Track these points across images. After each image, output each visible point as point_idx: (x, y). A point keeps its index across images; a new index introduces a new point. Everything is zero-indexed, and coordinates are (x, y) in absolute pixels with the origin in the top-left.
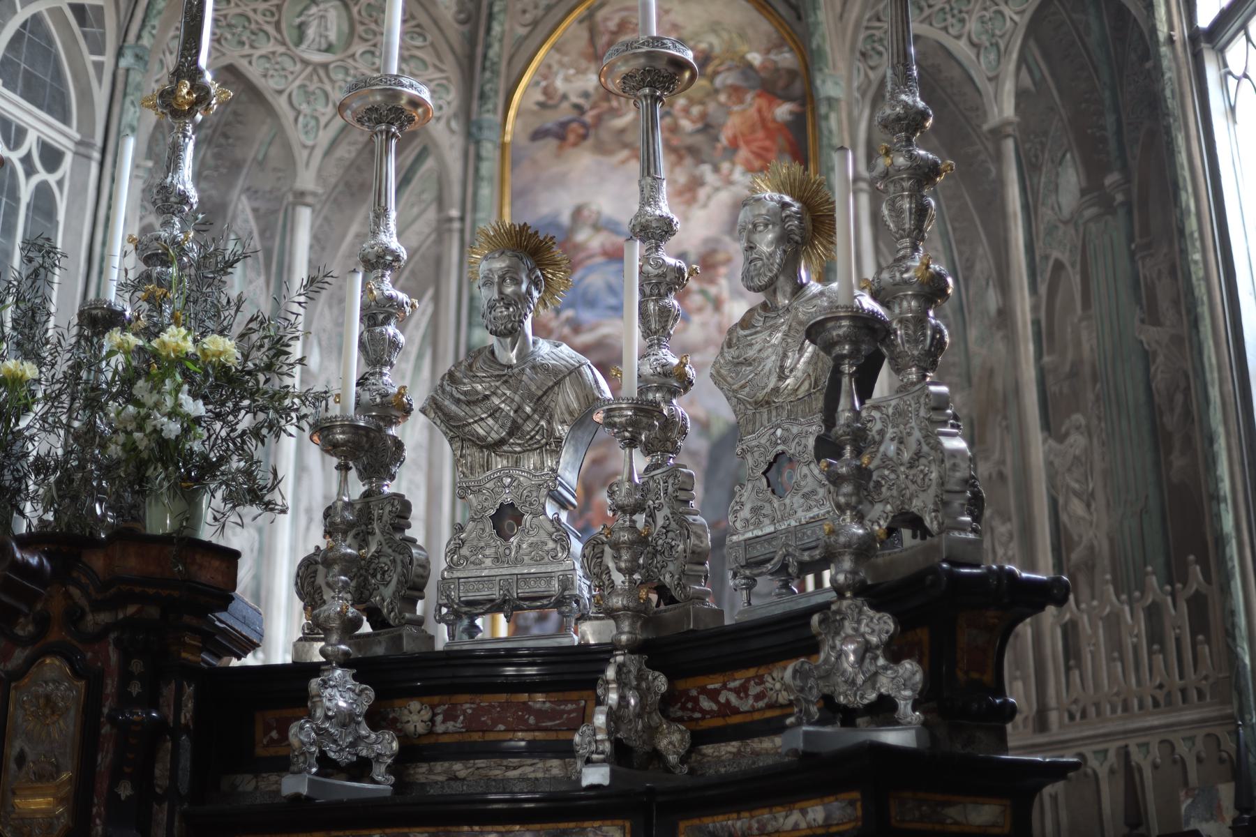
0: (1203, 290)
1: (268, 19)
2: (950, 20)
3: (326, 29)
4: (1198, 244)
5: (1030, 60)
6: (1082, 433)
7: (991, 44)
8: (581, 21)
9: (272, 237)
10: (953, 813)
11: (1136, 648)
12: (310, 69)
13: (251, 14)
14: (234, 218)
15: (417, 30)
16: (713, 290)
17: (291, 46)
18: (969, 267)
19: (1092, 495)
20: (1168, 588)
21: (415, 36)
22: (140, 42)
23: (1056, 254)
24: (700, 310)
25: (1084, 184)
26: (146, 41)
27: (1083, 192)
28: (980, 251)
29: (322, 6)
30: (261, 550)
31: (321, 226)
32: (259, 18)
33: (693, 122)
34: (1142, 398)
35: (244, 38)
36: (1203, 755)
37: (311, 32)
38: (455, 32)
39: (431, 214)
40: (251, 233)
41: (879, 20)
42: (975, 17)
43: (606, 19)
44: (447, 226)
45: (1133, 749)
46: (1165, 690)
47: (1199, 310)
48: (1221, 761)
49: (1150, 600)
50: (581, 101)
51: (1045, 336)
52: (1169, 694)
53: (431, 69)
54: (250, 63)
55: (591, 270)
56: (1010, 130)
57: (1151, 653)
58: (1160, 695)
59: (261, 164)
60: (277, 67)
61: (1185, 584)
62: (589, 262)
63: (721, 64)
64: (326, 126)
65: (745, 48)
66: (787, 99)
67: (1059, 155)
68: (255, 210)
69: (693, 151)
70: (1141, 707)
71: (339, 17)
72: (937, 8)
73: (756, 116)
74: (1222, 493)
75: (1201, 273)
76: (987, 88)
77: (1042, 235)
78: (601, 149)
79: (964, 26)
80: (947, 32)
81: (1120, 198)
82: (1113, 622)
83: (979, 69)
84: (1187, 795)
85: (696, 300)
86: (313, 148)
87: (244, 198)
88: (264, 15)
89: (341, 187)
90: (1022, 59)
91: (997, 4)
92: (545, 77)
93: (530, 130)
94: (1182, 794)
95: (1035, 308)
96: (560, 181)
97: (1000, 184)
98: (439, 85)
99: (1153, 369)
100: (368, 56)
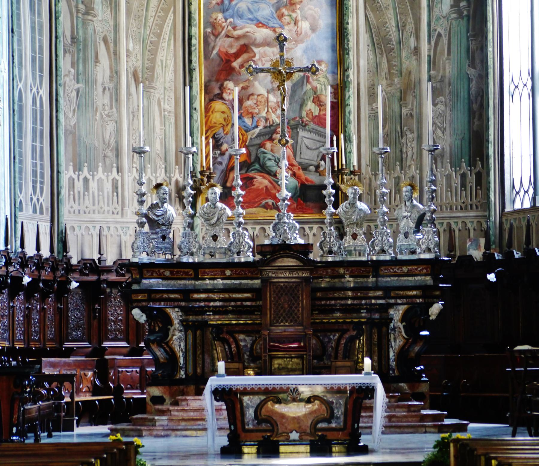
0: (492, 63)
4: (492, 44)
10: (434, 293)
11: (456, 188)
16: (294, 15)
18: (404, 26)
19: (445, 129)
20: (469, 168)
23: (439, 30)
24: (289, 24)
25: (452, 3)
27: (452, 6)
28: (409, 20)
34: (466, 96)
36: (476, 228)
45: (453, 224)
46: (465, 204)
47: (489, 70)
48: (482, 230)
49: (462, 172)
51: (432, 63)
52: (466, 206)
57: (461, 190)
58: (463, 206)
61: (475, 168)
70: (456, 209)
74: (490, 140)
75: (492, 56)
77: (434, 20)
81: (465, 13)
82: (449, 177)
84: (469, 241)
85: (287, 19)
94: (468, 240)
95: (429, 50)
99: (471, 86)
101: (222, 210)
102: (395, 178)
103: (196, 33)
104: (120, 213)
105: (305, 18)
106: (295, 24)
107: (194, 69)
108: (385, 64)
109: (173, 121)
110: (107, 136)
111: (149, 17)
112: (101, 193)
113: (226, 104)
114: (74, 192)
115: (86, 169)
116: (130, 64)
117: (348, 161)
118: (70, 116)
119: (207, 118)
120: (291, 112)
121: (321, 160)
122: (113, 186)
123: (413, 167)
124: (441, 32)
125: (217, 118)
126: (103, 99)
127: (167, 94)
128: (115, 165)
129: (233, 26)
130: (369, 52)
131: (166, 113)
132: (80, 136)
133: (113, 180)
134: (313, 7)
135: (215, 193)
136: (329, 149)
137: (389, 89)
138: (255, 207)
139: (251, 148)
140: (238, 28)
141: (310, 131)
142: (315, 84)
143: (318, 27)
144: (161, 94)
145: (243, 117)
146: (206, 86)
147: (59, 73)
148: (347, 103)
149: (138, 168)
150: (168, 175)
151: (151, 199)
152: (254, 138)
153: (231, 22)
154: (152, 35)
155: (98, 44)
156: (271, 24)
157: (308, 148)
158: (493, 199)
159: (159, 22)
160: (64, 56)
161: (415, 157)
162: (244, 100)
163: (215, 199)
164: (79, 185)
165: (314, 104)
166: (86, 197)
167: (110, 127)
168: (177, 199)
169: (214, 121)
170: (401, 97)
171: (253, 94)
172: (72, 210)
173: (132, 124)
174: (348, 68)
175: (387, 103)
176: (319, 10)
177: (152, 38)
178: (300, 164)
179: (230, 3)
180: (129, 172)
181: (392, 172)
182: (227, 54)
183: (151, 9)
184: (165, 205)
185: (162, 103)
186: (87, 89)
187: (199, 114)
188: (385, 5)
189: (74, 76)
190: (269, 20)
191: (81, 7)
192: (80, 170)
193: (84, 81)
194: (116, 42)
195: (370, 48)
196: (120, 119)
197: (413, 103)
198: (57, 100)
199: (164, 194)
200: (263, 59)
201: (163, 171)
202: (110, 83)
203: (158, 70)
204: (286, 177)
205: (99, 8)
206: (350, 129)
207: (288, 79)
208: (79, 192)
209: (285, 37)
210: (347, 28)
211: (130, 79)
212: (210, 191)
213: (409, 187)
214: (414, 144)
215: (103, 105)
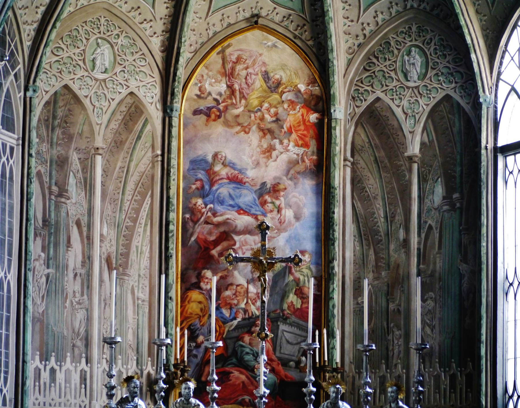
0: (485, 258)
1: (80, 58)
2: (395, 97)
3: (104, 61)
4: (485, 239)
5: (429, 130)
6: (432, 301)
7: (412, 116)
8: (218, 53)
9: (87, 172)
11: (445, 390)
12: (98, 82)
13: (73, 56)
14: (71, 164)
15: (142, 56)
17: (90, 71)
18: (393, 217)
19: (434, 327)
20: (459, 369)
22: (35, 84)
23: (430, 222)
24: (271, 211)
25: (444, 194)
26: (38, 83)
27: (444, 198)
28: (398, 211)
29: (102, 48)
30: (87, 319)
31: (106, 165)
33: (272, 117)
34: (457, 293)
35: (71, 70)
37: (98, 63)
38: (159, 56)
39: (150, 154)
40: (78, 171)
41: (362, 83)
42: (406, 99)
43: (231, 54)
44: (156, 159)
47: (482, 266)
50: (218, 97)
51: (422, 256)
54: (74, 83)
55: (222, 185)
56: (416, 159)
57: (450, 392)
59: (80, 135)
60: (85, 83)
62: (220, 182)
63: (286, 88)
64: (106, 113)
65: (297, 81)
66: (316, 111)
67: (436, 178)
68: (79, 159)
71: (109, 53)
72: (390, 88)
73: (301, 117)
74: (482, 340)
75: (485, 251)
76: (409, 136)
77: (425, 212)
78: (227, 124)
79: (401, 102)
80: (393, 101)
81: (458, 205)
82: (437, 378)
83: (407, 127)
85: (270, 206)
86: (101, 124)
87: (74, 153)
88: (78, 56)
89: (113, 144)
90: (425, 128)
91: (417, 97)
92: (200, 82)
93: (193, 109)
95: (419, 243)
96: (207, 138)
97: (409, 183)
100: (122, 73)
101: (195, 406)
102: (380, 377)
103: (174, 219)
106: (278, 212)
107: (171, 256)
108: (372, 257)
109: (147, 310)
110: (77, 325)
111: (125, 201)
112: (68, 385)
113: (203, 294)
114: (39, 383)
115: (53, 359)
116: (104, 249)
117: (330, 357)
118: (39, 302)
119: (183, 308)
120: (271, 304)
121: (302, 356)
122: (81, 378)
123: (400, 366)
124: (431, 223)
125: (193, 308)
126: (74, 285)
127: (142, 281)
128: (84, 355)
129: (213, 212)
130: (356, 243)
131: (140, 302)
132: (48, 324)
133: (81, 371)
134: (297, 195)
135: (189, 388)
136: (310, 344)
137: (376, 282)
138: (231, 404)
139: (228, 341)
140: (218, 214)
141: (291, 325)
142: (298, 275)
143: (303, 215)
144: (136, 282)
145: (221, 308)
146: (182, 274)
147: (28, 257)
148: (331, 296)
149: (108, 359)
150: (140, 367)
151: (121, 393)
152: (232, 330)
153: (210, 208)
154: (127, 220)
155: (71, 228)
156: (253, 211)
157: (288, 342)
158: (484, 403)
159: (136, 206)
160: (35, 240)
161: (401, 355)
162: (222, 290)
163: (189, 394)
164: (45, 376)
165: (296, 297)
166: (53, 389)
167: (81, 315)
168: (149, 393)
169: (190, 311)
170: (388, 291)
171: (232, 284)
172: (37, 402)
173: (104, 312)
174: (333, 259)
175: (373, 297)
176: (304, 198)
177: (128, 222)
178: (279, 359)
179: (210, 189)
180: (99, 363)
181: (378, 371)
182: (206, 241)
183: (127, 192)
184: (136, 399)
185: (136, 291)
186: (58, 275)
187: (174, 303)
188: (373, 195)
189: (44, 261)
190: (251, 207)
191: (55, 188)
192: (47, 360)
193: (54, 266)
194: (90, 226)
195: (357, 239)
196: (91, 307)
197: (400, 298)
198: (25, 286)
199: (134, 388)
200: (243, 247)
201: (135, 363)
202: (82, 269)
203: (133, 256)
204: (265, 373)
205: (73, 190)
206: (334, 323)
207: (269, 269)
208: (45, 383)
209: (267, 226)
210: (333, 218)
211: (103, 265)
212: (184, 386)
213: (395, 388)
214: (401, 341)
215: (74, 292)
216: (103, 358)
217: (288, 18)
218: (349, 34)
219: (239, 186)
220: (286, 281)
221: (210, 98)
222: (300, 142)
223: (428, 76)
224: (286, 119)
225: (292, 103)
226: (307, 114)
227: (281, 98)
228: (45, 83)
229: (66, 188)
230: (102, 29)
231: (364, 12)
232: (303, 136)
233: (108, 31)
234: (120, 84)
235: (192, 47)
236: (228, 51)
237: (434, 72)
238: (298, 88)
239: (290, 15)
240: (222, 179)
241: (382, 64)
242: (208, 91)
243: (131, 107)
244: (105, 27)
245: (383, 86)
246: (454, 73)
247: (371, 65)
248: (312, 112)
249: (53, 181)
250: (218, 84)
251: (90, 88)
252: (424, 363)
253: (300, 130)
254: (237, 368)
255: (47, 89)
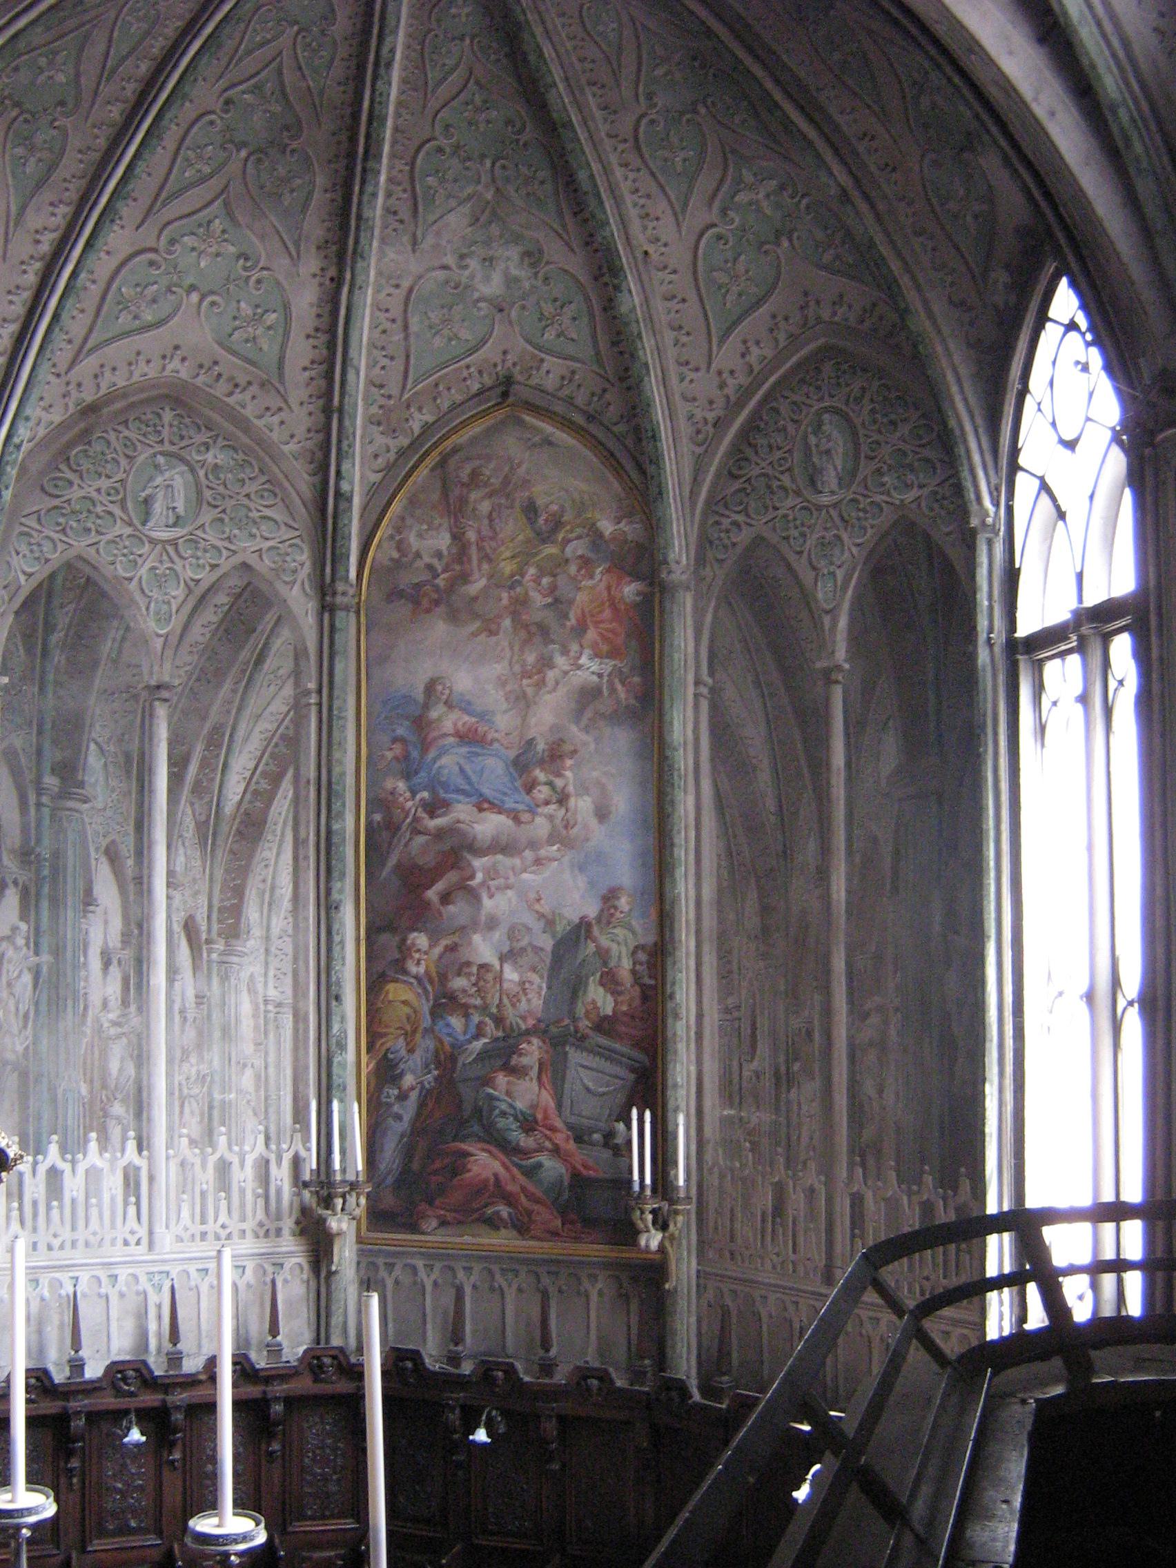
13: (94, 495)
16: (559, 783)
21: (266, 494)
24: (547, 803)
29: (167, 475)
32: (104, 498)
35: (90, 525)
37: (158, 507)
39: (288, 690)
41: (727, 507)
44: (304, 701)
50: (435, 562)
53: (283, 528)
54: (98, 551)
60: (125, 551)
63: (572, 531)
66: (637, 577)
69: (544, 630)
72: (780, 512)
73: (605, 594)
78: (453, 617)
85: (542, 792)
98: (291, 546)
104: (145, 1241)
105: (584, 789)
115: (53, 1149)
116: (176, 902)
121: (617, 1121)
123: (812, 1166)
126: (105, 984)
128: (132, 1134)
131: (270, 1007)
133: (125, 1169)
141: (596, 1051)
142: (604, 941)
143: (613, 809)
155: (93, 862)
156: (510, 804)
165: (601, 990)
166: (55, 1213)
185: (260, 987)
189: (28, 939)
191: (50, 781)
192: (38, 1151)
200: (491, 883)
201: (261, 1138)
208: (35, 1203)
216: (180, 1136)
217: (570, 381)
218: (694, 399)
219: (478, 750)
220: (581, 957)
221: (419, 564)
222: (605, 648)
223: (860, 476)
224: (574, 599)
225: (585, 563)
226: (618, 585)
227: (563, 551)
228: (24, 556)
229: (80, 778)
230: (166, 433)
231: (722, 342)
232: (610, 635)
233: (182, 438)
234: (214, 547)
235: (380, 460)
236: (452, 463)
237: (873, 465)
238: (597, 529)
239: (573, 372)
240: (446, 735)
241: (764, 460)
242: (414, 550)
243: (240, 595)
244: (175, 429)
245: (766, 508)
246: (916, 464)
247: (743, 463)
248: (628, 579)
249: (47, 766)
250: (434, 533)
251: (140, 561)
252: (863, 1165)
253: (602, 622)
254: (480, 1145)
255: (29, 570)
